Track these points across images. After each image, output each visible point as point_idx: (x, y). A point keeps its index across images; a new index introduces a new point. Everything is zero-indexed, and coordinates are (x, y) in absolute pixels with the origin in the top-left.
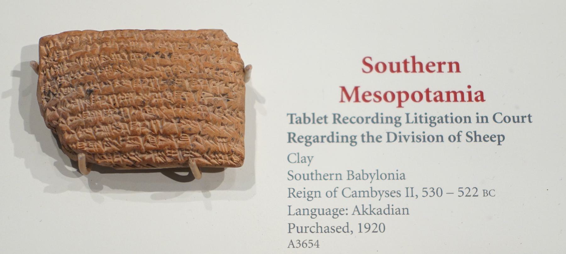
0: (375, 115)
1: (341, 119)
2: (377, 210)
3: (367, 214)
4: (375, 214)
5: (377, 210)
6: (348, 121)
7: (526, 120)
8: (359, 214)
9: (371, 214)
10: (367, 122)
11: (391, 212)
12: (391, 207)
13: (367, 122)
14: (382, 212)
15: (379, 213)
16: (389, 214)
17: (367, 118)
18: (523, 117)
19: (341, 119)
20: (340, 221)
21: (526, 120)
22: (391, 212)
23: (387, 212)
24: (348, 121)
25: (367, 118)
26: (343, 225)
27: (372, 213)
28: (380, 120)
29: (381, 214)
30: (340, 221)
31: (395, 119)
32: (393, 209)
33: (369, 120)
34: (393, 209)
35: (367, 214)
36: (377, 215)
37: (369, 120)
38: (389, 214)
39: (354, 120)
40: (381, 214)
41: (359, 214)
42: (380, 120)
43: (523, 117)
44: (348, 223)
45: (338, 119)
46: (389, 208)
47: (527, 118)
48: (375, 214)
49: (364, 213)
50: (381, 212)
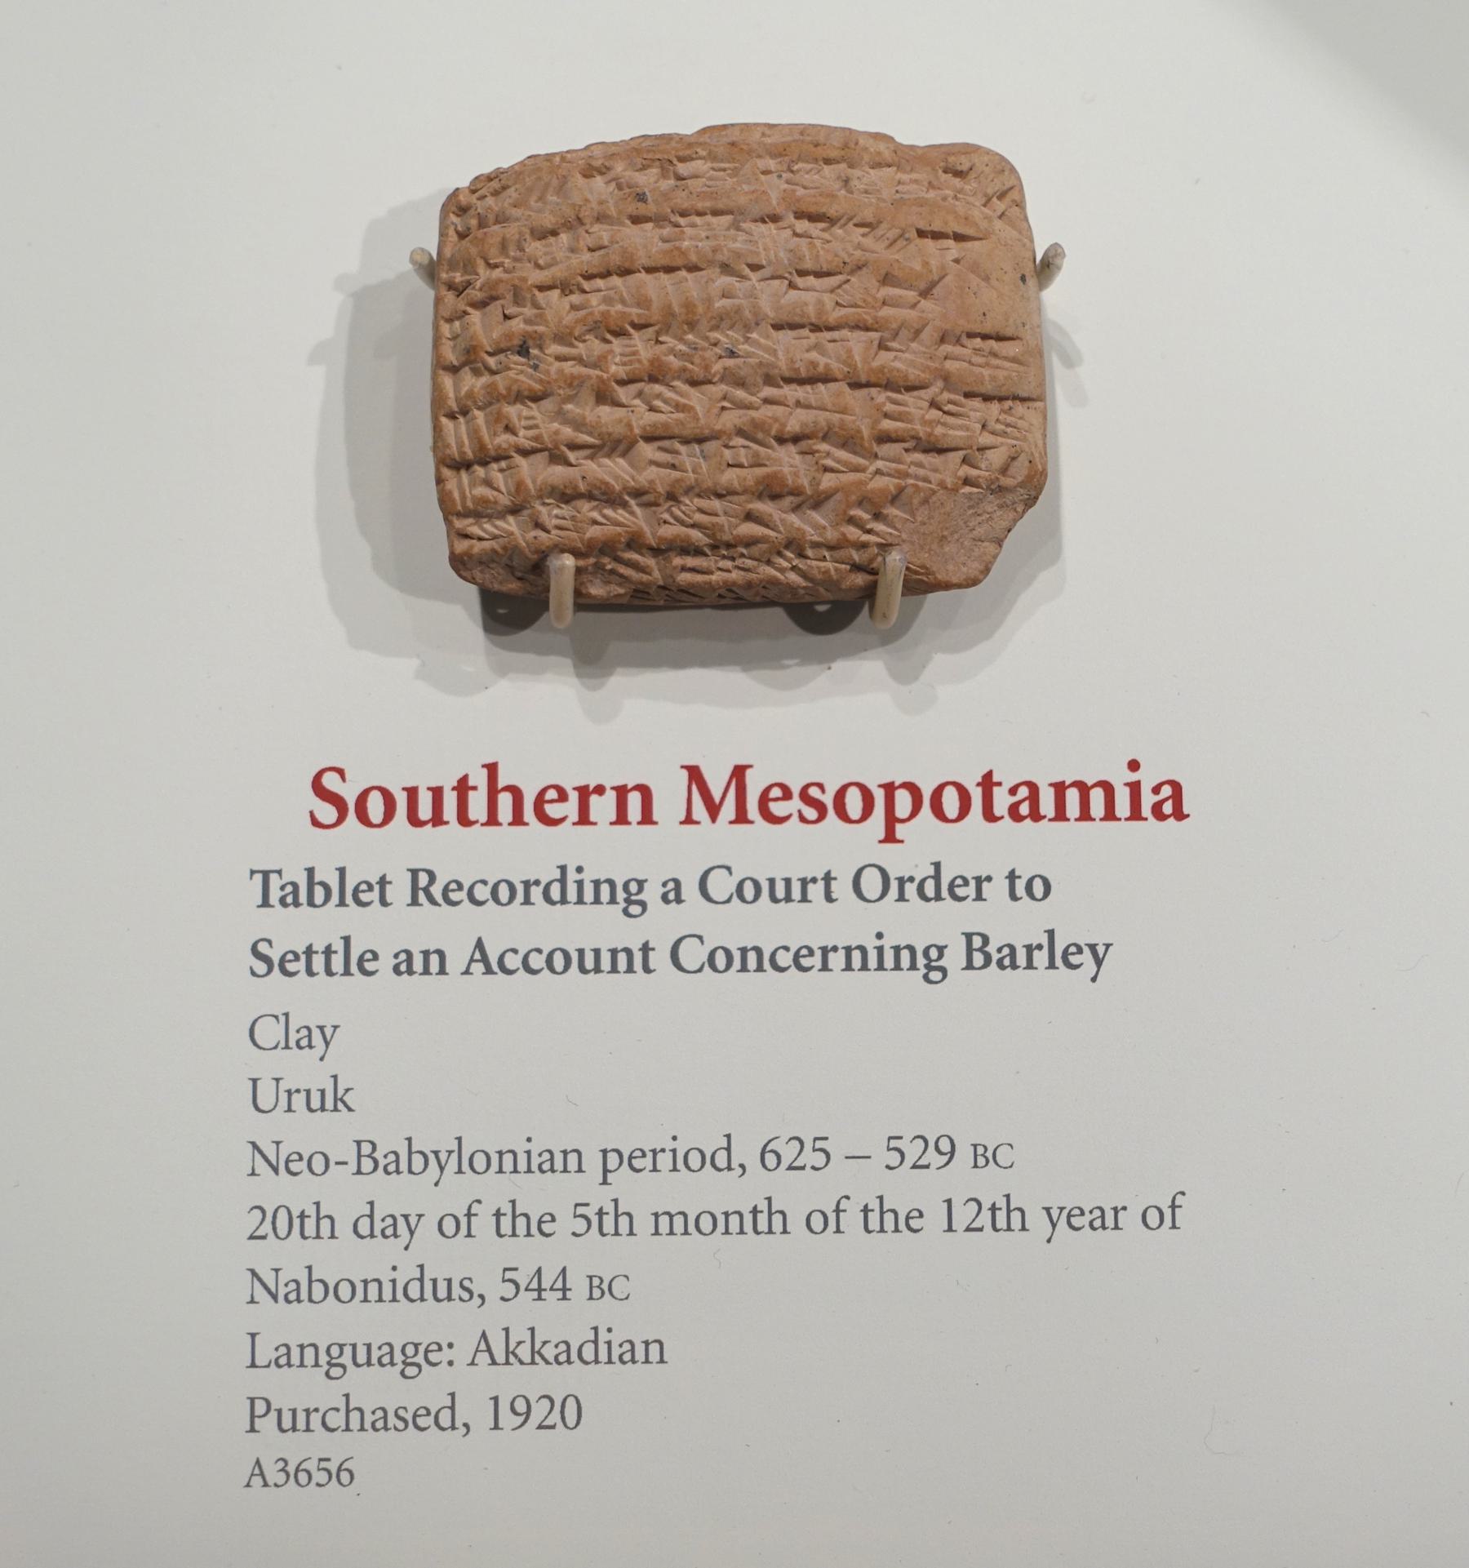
0: (557, 874)
1: (436, 891)
2: (556, 1346)
3: (521, 1362)
4: (547, 1362)
5: (556, 1346)
6: (462, 896)
7: (816, 891)
8: (494, 1362)
9: (533, 1362)
10: (527, 901)
11: (603, 1356)
12: (603, 1336)
13: (527, 901)
14: (574, 1356)
15: (563, 1358)
16: (597, 1361)
17: (527, 885)
18: (804, 882)
19: (436, 891)
20: (428, 1389)
21: (816, 891)
22: (603, 1356)
23: (588, 1353)
24: (462, 896)
25: (527, 885)
26: (439, 1401)
27: (537, 1358)
28: (572, 894)
29: (569, 1361)
30: (428, 1389)
31: (626, 886)
32: (609, 1343)
33: (536, 893)
34: (609, 1343)
35: (521, 1362)
36: (555, 1366)
37: (536, 893)
38: (597, 1361)
39: (482, 893)
40: (569, 1361)
41: (494, 1362)
42: (572, 894)
43: (804, 882)
44: (453, 1395)
45: (426, 890)
46: (596, 1342)
47: (821, 884)
48: (547, 1362)
49: (512, 1359)
50: (567, 1355)
